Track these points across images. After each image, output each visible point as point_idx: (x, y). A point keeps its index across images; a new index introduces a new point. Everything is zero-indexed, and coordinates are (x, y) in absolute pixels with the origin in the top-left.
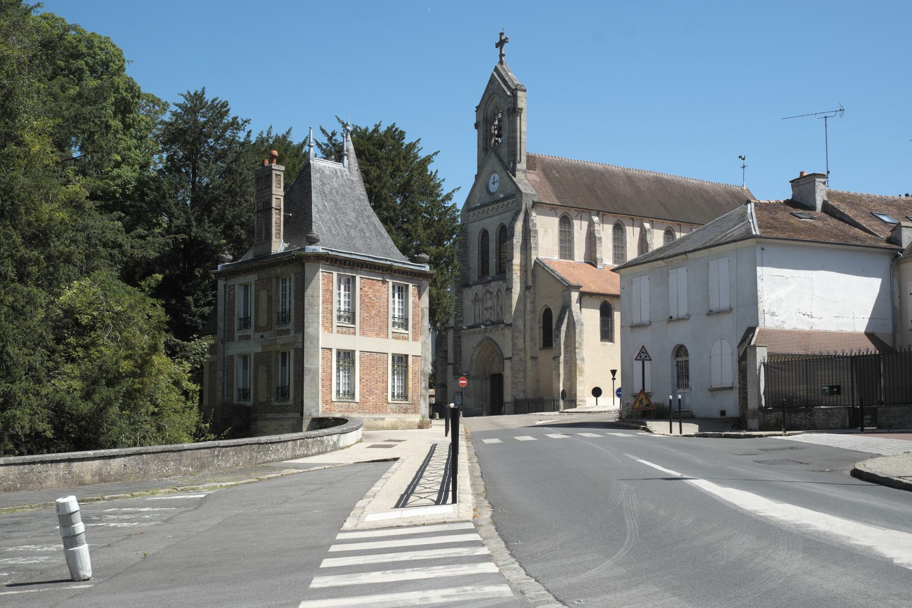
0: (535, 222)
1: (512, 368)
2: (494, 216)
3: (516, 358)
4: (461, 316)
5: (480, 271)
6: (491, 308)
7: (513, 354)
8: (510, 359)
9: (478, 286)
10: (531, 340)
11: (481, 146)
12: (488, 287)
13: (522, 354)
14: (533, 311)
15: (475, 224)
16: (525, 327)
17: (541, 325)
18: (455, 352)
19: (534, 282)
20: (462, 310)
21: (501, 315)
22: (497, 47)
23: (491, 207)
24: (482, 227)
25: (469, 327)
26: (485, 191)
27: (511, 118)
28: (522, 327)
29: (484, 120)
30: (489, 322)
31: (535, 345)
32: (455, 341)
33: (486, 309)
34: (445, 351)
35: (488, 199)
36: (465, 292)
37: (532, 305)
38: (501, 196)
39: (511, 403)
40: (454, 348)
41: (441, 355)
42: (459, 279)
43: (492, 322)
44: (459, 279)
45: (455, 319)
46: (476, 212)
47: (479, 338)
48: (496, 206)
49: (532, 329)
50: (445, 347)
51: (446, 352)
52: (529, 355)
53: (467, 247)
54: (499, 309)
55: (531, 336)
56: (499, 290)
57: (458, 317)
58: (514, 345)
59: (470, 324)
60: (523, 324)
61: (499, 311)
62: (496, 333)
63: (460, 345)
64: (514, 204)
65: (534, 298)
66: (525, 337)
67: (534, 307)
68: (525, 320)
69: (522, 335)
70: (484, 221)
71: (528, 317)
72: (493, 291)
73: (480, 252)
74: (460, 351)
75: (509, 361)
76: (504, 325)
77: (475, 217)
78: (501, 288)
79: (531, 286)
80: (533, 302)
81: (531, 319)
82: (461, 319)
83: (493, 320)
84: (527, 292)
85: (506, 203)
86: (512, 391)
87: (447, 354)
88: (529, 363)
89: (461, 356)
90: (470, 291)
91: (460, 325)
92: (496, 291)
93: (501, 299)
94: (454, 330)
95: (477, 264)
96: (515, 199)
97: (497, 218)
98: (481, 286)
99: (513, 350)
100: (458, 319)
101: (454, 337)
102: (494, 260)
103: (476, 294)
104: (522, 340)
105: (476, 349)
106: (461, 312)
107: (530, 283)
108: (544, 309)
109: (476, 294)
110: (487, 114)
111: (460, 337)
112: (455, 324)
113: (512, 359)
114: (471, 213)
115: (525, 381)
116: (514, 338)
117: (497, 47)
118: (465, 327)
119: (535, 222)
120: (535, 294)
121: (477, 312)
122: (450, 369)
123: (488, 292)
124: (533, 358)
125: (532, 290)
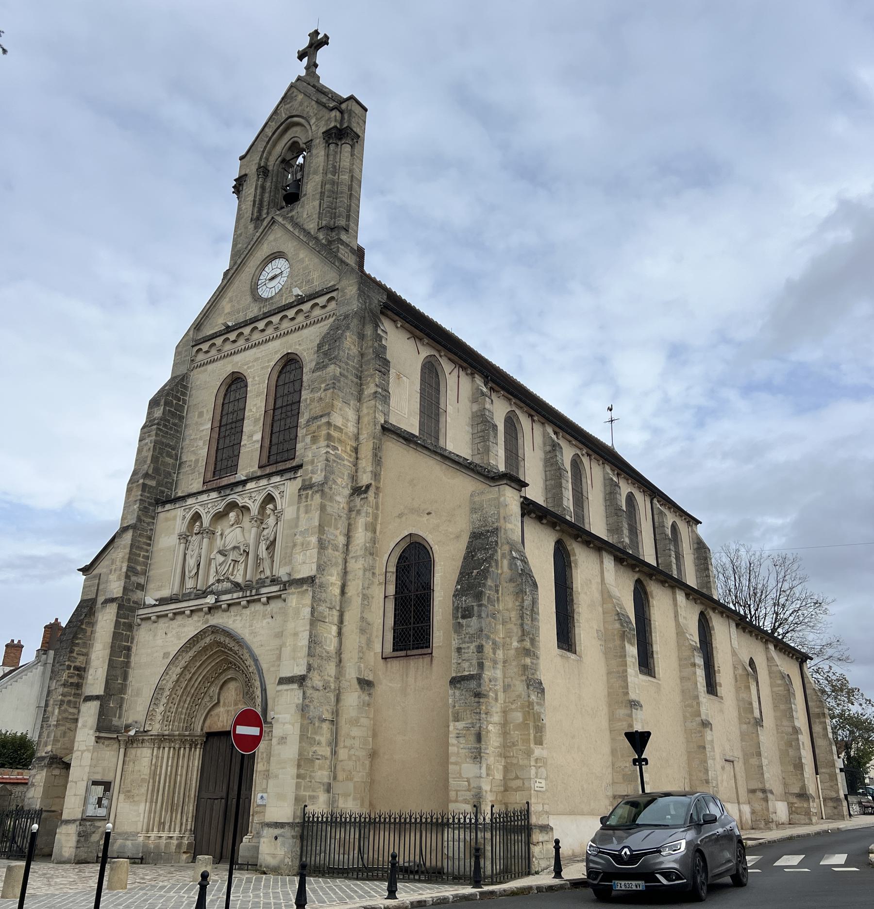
0: (384, 342)
1: (303, 709)
2: (267, 341)
3: (316, 680)
4: (144, 573)
5: (211, 468)
6: (235, 548)
7: (310, 668)
8: (301, 680)
9: (204, 497)
10: (363, 631)
11: (248, 215)
12: (230, 498)
13: (331, 669)
14: (371, 551)
15: (210, 367)
16: (343, 592)
17: (391, 590)
18: (111, 665)
19: (376, 475)
20: (147, 558)
21: (266, 564)
22: (301, 57)
23: (261, 325)
24: (229, 369)
25: (162, 601)
26: (249, 299)
27: (332, 147)
28: (337, 591)
29: (260, 167)
30: (227, 585)
31: (369, 642)
32: (116, 636)
33: (222, 552)
34: (77, 668)
35: (254, 311)
36: (162, 516)
37: (369, 534)
38: (297, 291)
39: (291, 825)
40: (111, 655)
41: (65, 676)
42: (153, 483)
43: (237, 585)
44: (153, 483)
45: (127, 577)
46: (219, 341)
47: (191, 627)
48: (275, 319)
49: (365, 597)
50: (81, 658)
51: (81, 671)
52: (351, 673)
53: (181, 418)
54: (263, 546)
55: (362, 618)
56: (270, 499)
57: (136, 573)
58: (314, 641)
59: (166, 593)
60: (339, 583)
61: (263, 552)
62: (247, 612)
63: (129, 649)
64: (333, 305)
65: (376, 517)
66: (341, 621)
67: (374, 541)
68: (345, 573)
69: (336, 613)
70: (237, 358)
71: (356, 566)
72: (249, 504)
73: (217, 424)
74: (127, 664)
75: (295, 686)
76: (275, 588)
77: (213, 352)
78: (276, 494)
79: (368, 487)
80: (372, 528)
81: (365, 570)
82: (141, 580)
83: (239, 579)
84: (358, 501)
85: (306, 307)
86: (298, 786)
87: (81, 677)
88: (352, 698)
89: (125, 677)
90: (180, 512)
91: (139, 595)
92: (258, 504)
93: (271, 521)
94: (120, 607)
95: (204, 452)
96: (334, 294)
97: (276, 344)
98: (214, 495)
99: (310, 655)
100: (133, 578)
101: (117, 624)
102: (258, 437)
103: (197, 517)
104: (334, 629)
105: (176, 657)
106: (146, 564)
107: (365, 479)
108: (404, 545)
109: (197, 517)
110: (267, 159)
111: (130, 627)
112: (125, 589)
113: (308, 683)
114: (205, 347)
115: (334, 753)
116: (315, 619)
117: (301, 57)
118: (150, 601)
119: (384, 342)
120: (377, 508)
121: (191, 562)
122: (89, 713)
123: (233, 506)
124: (365, 684)
125: (371, 493)
